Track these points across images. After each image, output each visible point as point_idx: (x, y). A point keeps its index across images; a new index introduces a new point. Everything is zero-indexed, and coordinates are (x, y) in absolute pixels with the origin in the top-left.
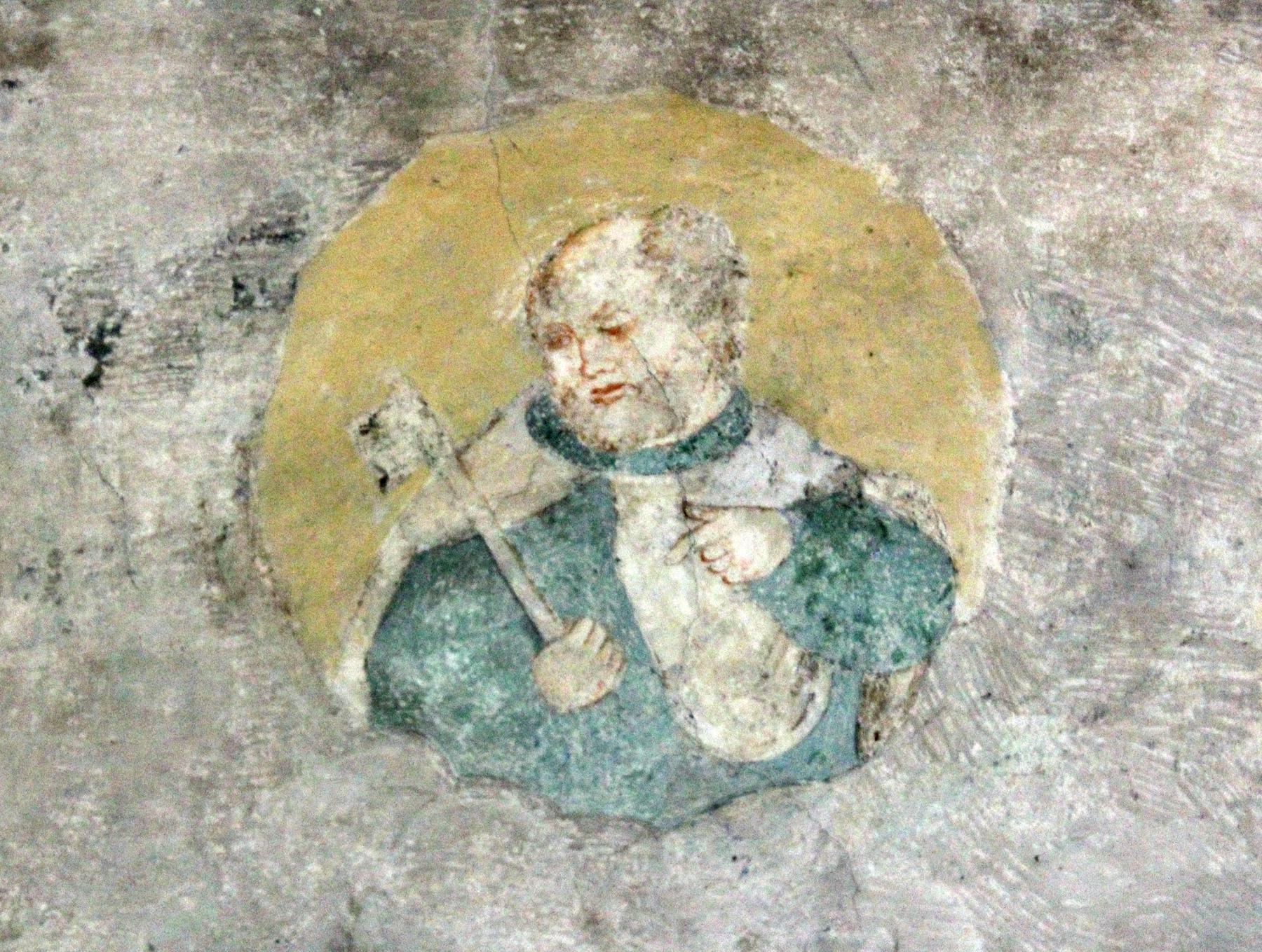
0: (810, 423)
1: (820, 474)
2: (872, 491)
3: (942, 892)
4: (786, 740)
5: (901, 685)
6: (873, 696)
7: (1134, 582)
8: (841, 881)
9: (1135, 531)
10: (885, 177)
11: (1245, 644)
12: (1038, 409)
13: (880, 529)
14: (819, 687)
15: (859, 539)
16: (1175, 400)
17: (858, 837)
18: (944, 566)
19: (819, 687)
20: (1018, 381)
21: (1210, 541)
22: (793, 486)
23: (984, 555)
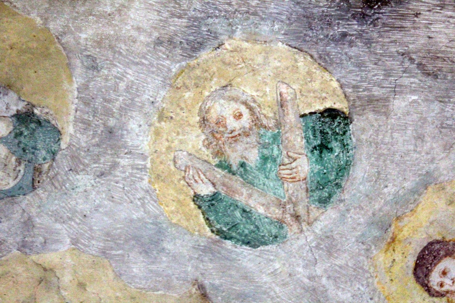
0: (17, 92)
1: (21, 106)
2: (36, 111)
3: (58, 226)
4: (12, 184)
5: (46, 167)
6: (38, 171)
7: (111, 137)
8: (28, 224)
9: (112, 122)
10: (39, 21)
11: (142, 154)
12: (84, 87)
13: (39, 123)
14: (22, 168)
15: (33, 126)
16: (122, 85)
17: (33, 211)
18: (57, 133)
19: (22, 168)
20: (77, 81)
21: (133, 125)
22: (14, 110)
23: (69, 130)
